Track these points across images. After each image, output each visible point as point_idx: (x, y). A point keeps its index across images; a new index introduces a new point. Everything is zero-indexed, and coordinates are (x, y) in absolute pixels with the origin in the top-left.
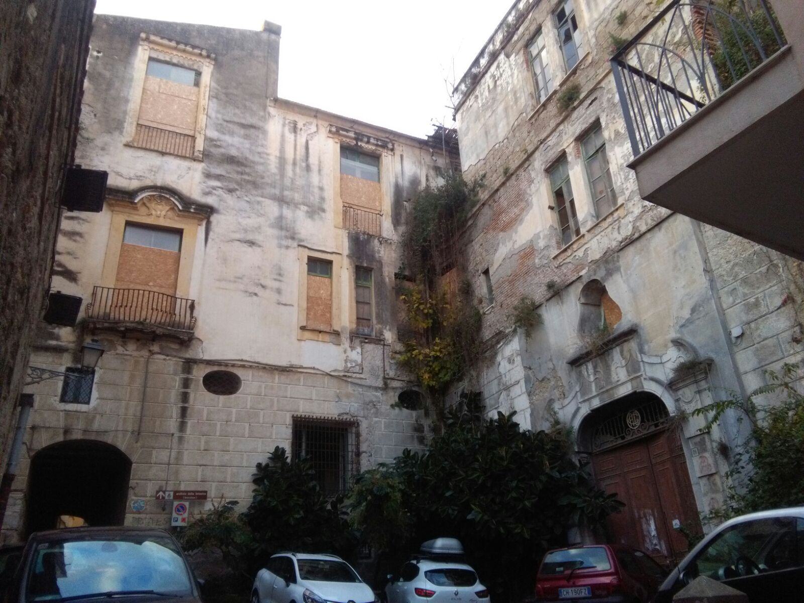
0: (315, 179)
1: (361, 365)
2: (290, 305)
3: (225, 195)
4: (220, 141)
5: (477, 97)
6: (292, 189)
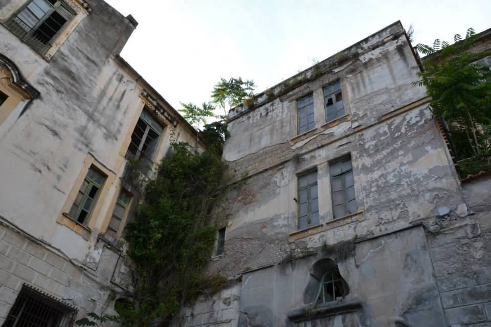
0: (119, 116)
1: (98, 264)
2: (63, 192)
3: (53, 92)
4: (68, 58)
5: (249, 117)
6: (101, 114)
